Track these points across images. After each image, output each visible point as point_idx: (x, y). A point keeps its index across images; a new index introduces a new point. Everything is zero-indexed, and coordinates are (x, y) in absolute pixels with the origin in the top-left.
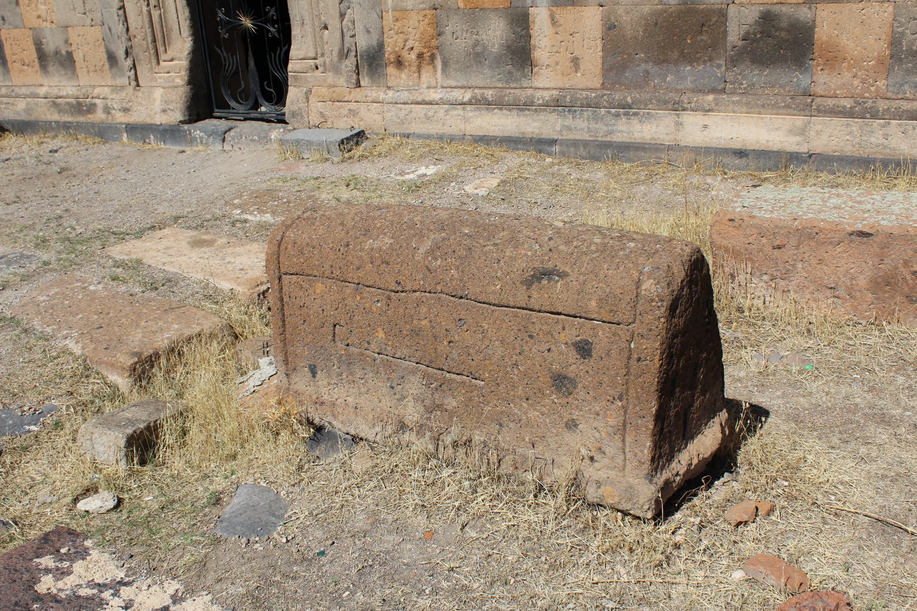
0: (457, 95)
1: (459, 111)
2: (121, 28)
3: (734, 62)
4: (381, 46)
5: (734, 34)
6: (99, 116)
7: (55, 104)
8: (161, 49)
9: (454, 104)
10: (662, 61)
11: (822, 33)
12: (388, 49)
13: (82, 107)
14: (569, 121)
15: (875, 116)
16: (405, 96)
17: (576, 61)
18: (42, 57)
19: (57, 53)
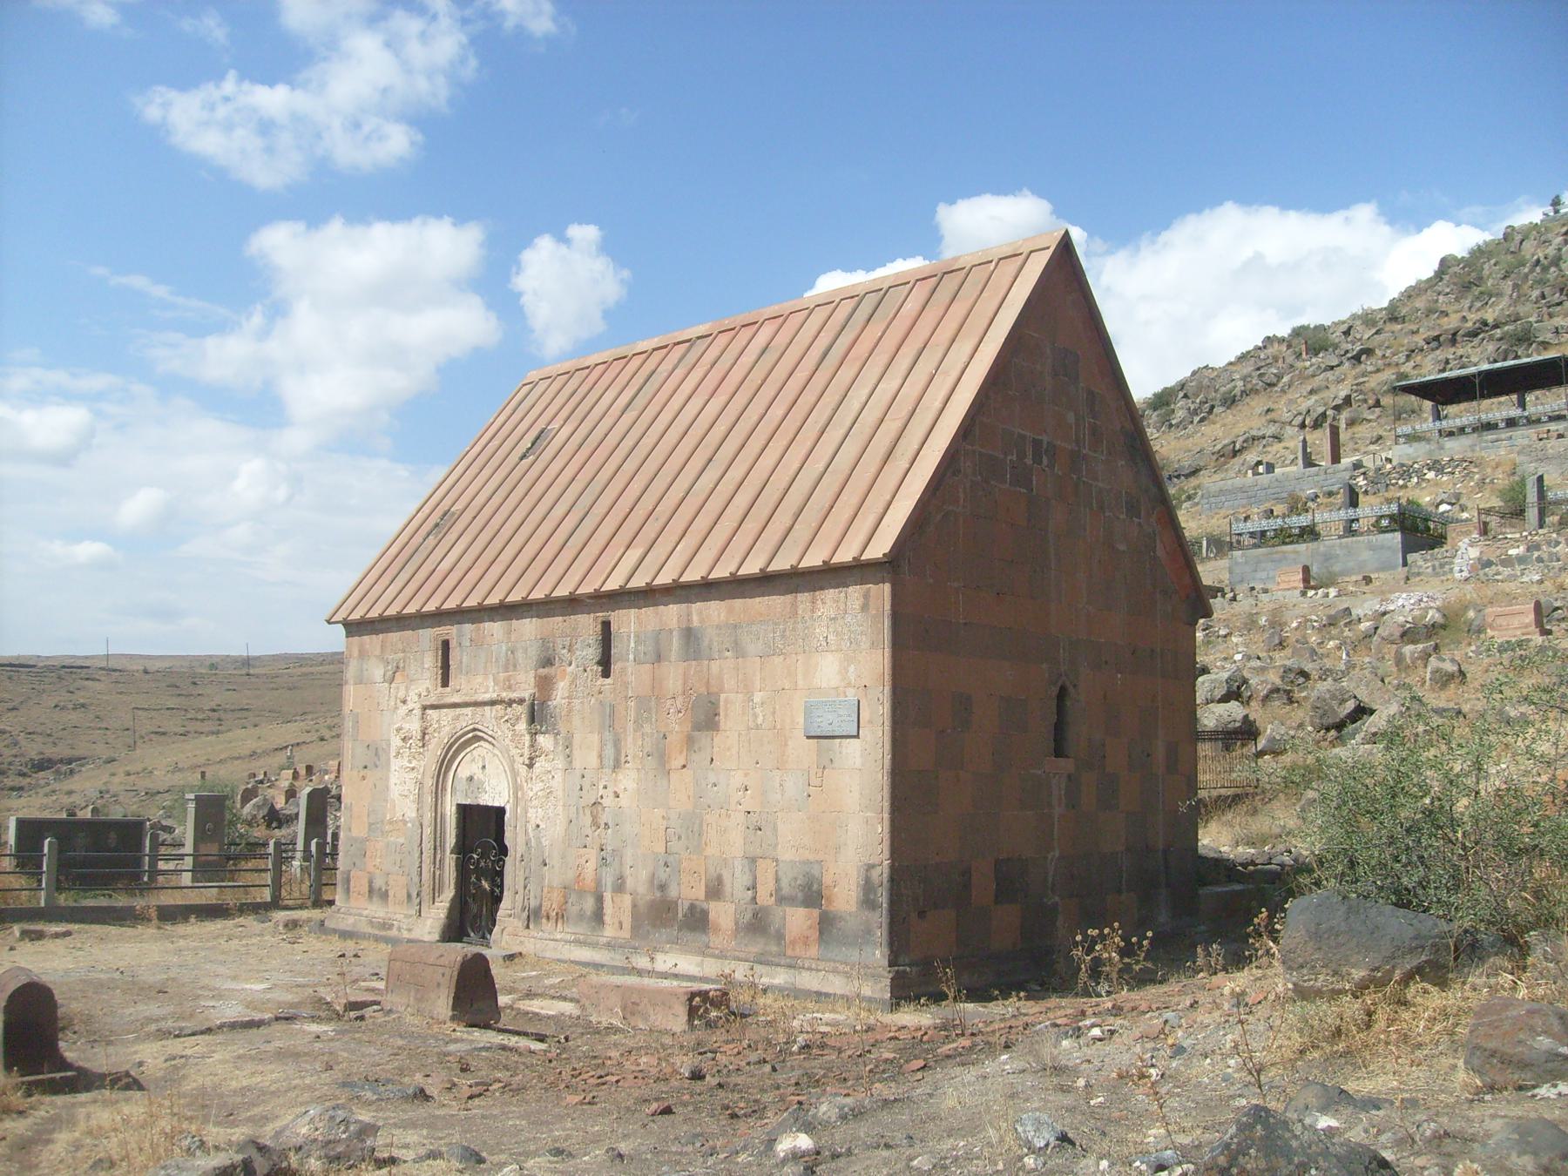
0: (568, 937)
1: (567, 947)
2: (416, 879)
3: (680, 930)
4: (541, 906)
5: (680, 915)
6: (394, 933)
7: (371, 922)
8: (437, 894)
9: (566, 942)
10: (654, 926)
11: (712, 916)
12: (543, 908)
13: (386, 926)
14: (612, 954)
15: (726, 958)
16: (546, 935)
17: (621, 924)
18: (371, 891)
19: (380, 889)
